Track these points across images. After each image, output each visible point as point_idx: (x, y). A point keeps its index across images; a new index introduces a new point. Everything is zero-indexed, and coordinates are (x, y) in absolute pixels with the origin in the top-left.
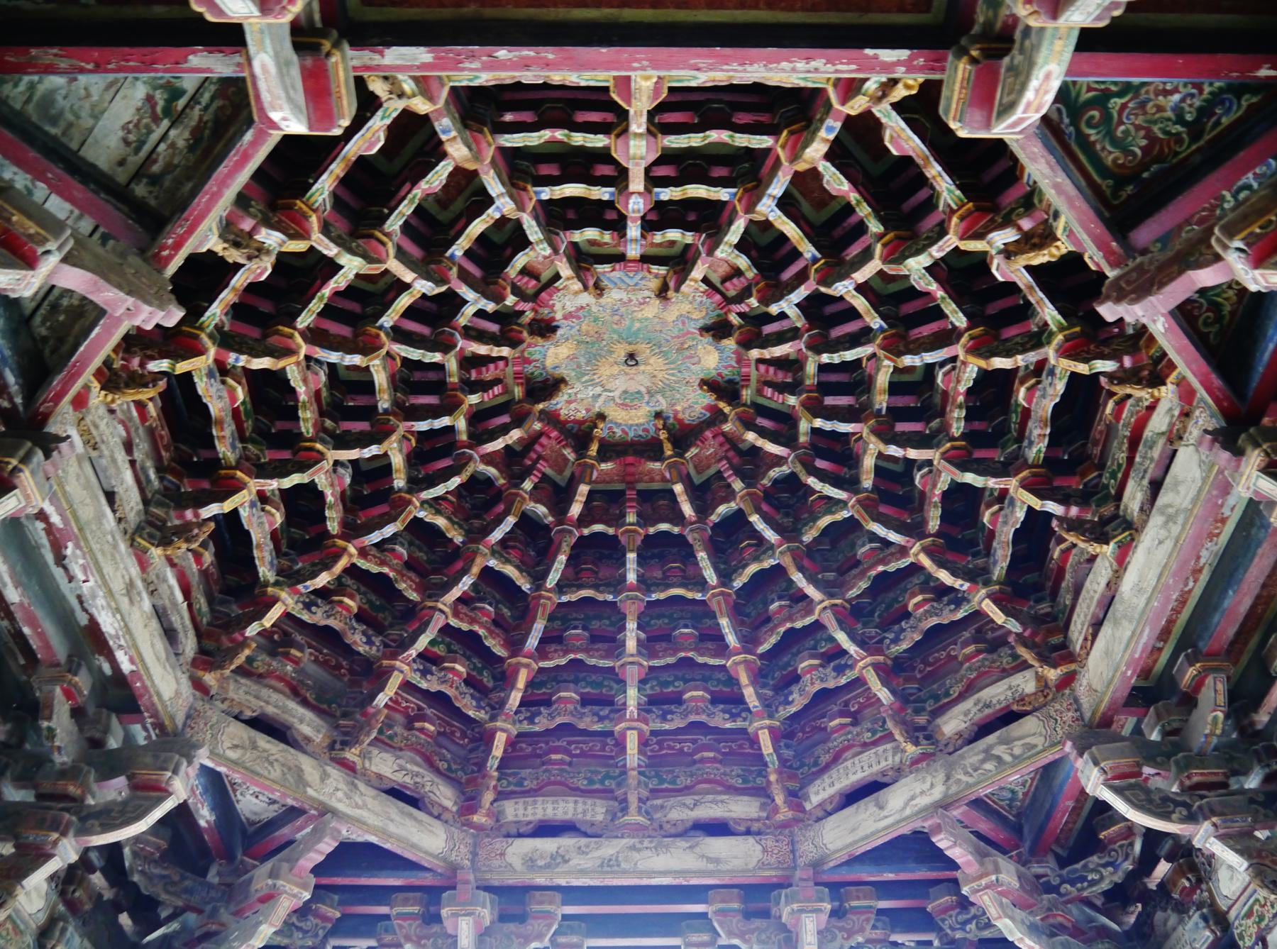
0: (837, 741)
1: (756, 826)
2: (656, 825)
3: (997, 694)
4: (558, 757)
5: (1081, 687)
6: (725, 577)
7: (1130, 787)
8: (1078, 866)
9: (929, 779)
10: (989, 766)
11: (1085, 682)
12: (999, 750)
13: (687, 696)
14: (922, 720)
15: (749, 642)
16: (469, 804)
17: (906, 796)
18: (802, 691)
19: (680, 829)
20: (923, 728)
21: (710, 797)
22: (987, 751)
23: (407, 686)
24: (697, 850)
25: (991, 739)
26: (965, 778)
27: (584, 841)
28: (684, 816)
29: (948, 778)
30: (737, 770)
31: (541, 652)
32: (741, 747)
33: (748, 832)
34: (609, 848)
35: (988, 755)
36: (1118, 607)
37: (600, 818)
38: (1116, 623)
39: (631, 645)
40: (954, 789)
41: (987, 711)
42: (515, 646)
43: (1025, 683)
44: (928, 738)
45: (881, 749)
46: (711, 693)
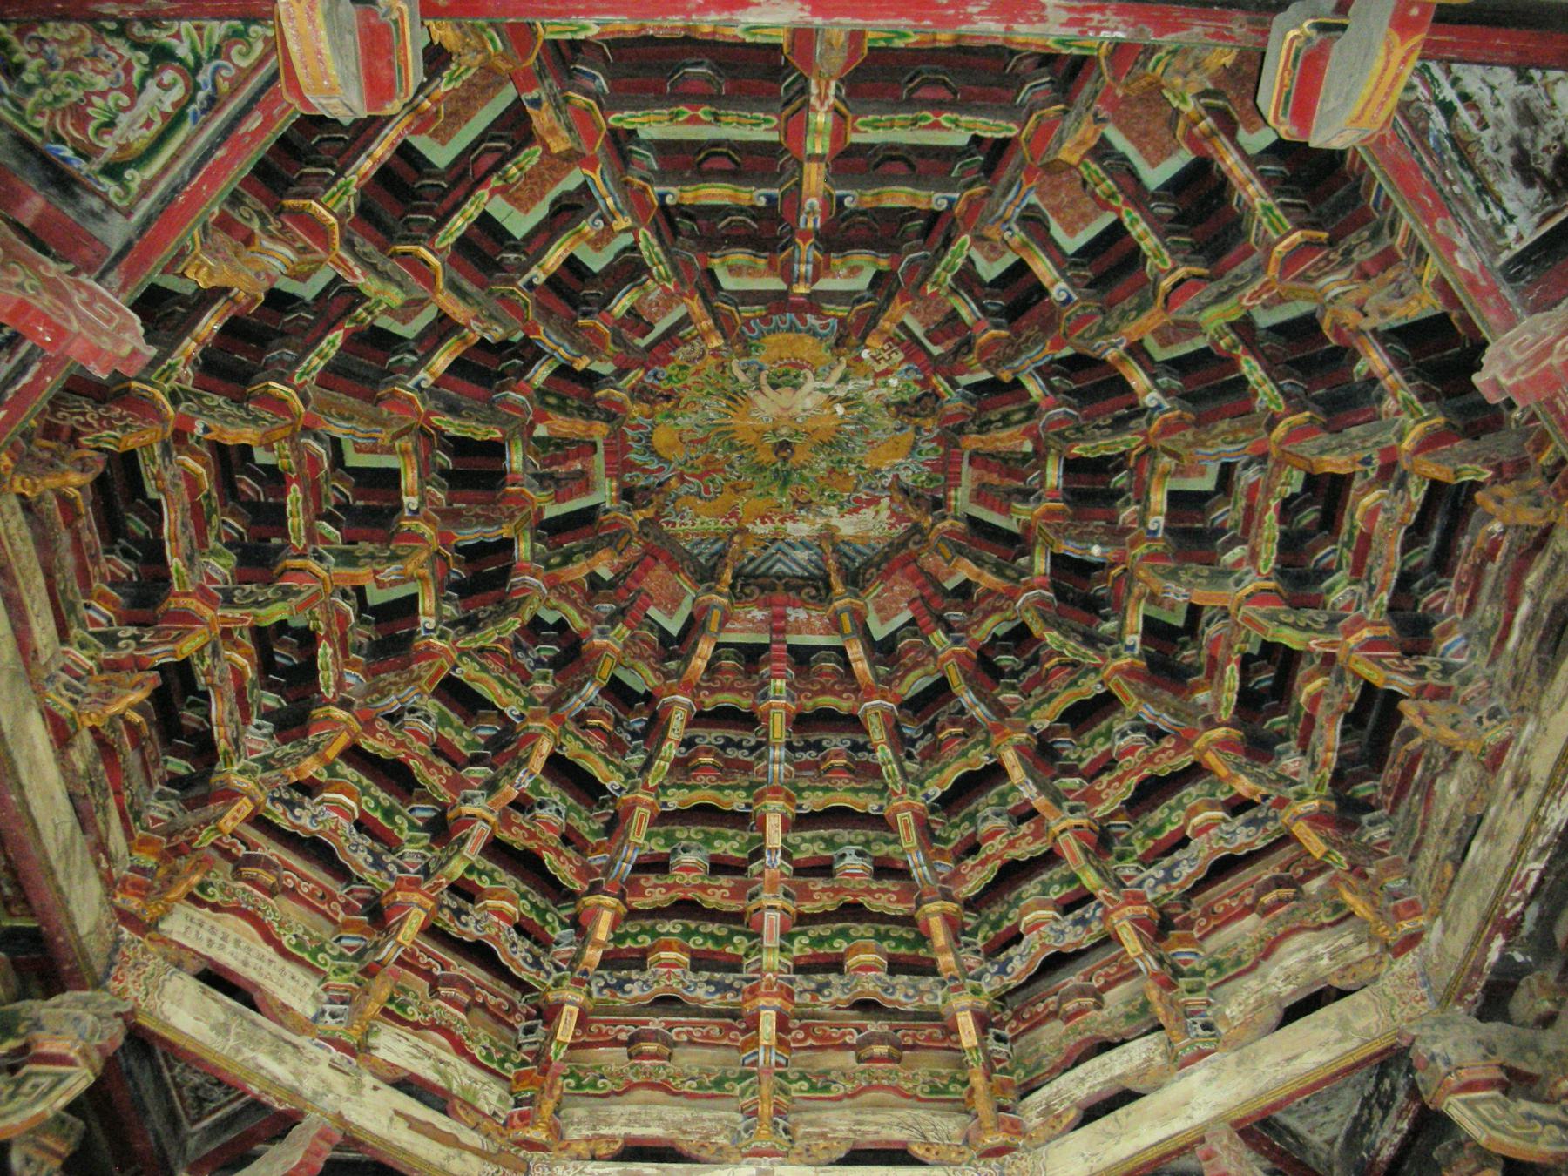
4: (651, 1047)
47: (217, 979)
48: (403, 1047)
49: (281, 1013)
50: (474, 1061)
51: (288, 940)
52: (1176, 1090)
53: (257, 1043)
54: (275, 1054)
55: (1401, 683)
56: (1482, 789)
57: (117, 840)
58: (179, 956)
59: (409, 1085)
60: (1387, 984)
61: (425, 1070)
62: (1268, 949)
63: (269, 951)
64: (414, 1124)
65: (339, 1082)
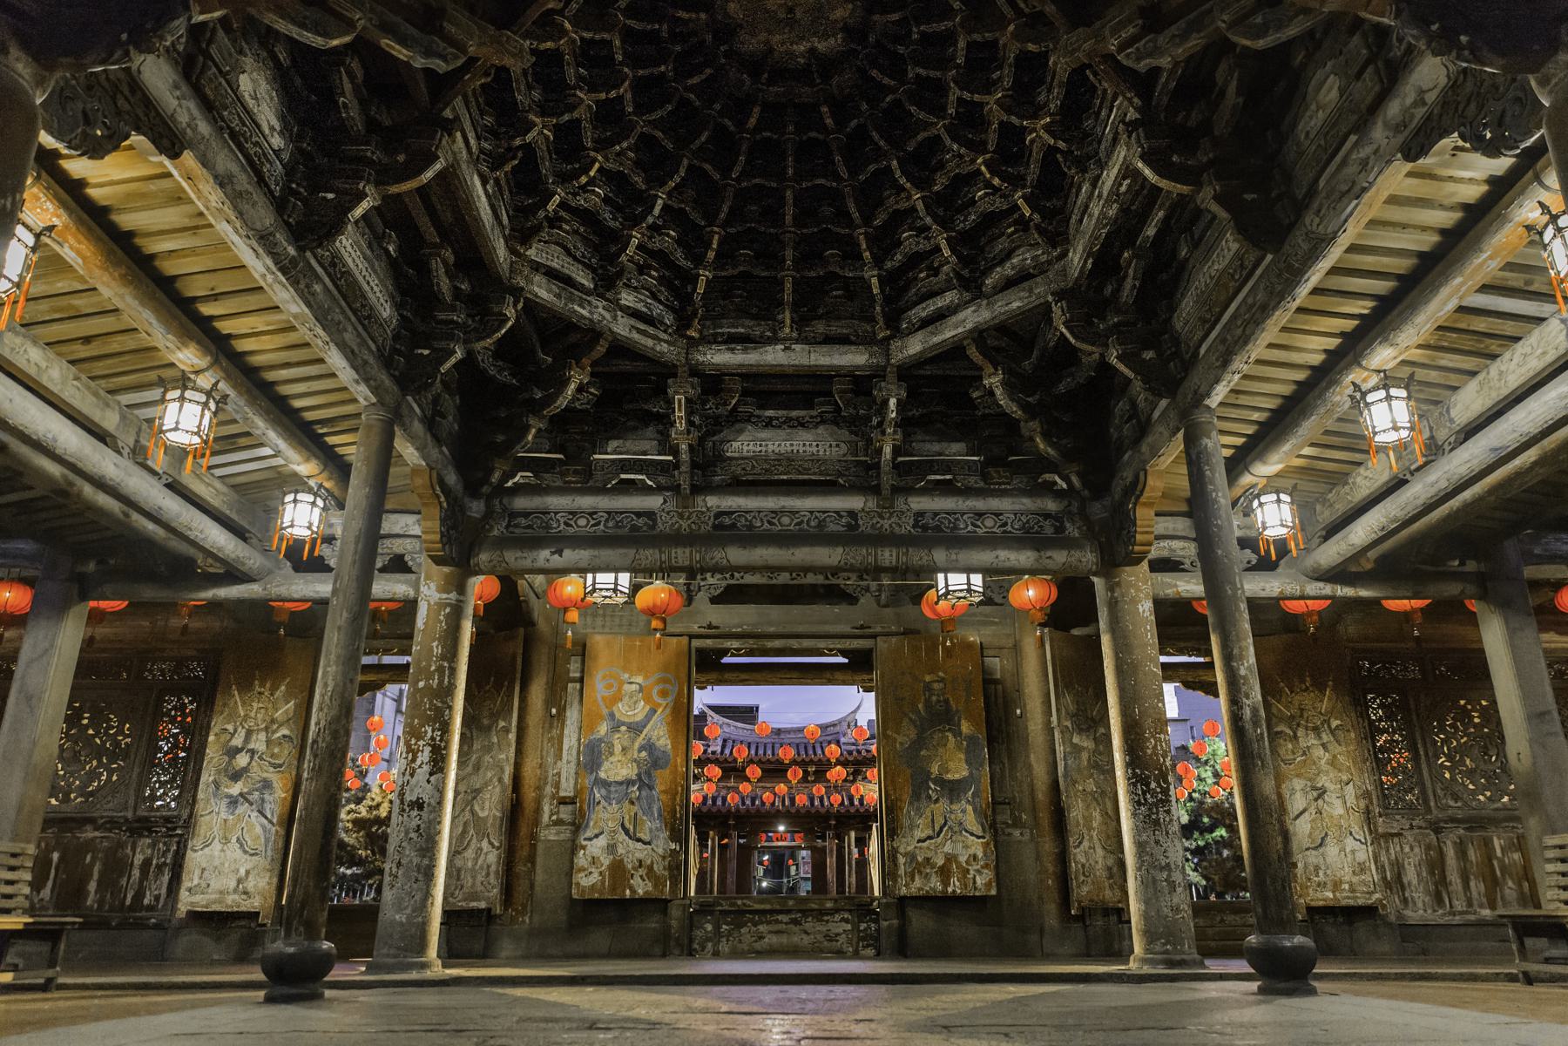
6: (853, 173)
15: (867, 220)
16: (683, 322)
23: (640, 247)
31: (726, 224)
39: (789, 219)
42: (711, 219)
47: (552, 274)
48: (631, 298)
49: (580, 288)
50: (660, 302)
51: (578, 254)
52: (961, 316)
53: (573, 301)
54: (581, 306)
55: (1061, 145)
56: (1090, 197)
57: (505, 220)
58: (536, 267)
59: (634, 314)
60: (1051, 275)
61: (641, 307)
62: (1009, 255)
63: (570, 260)
64: (639, 331)
65: (607, 315)
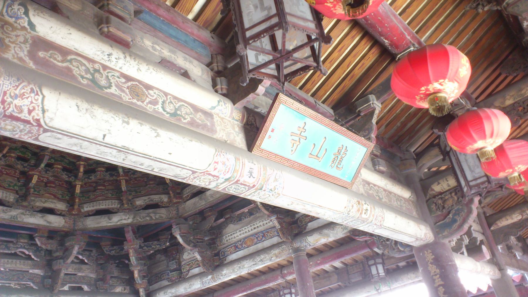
0: (98, 193)
1: (63, 213)
2: (31, 206)
3: (156, 198)
5: (181, 207)
7: (184, 236)
8: (151, 243)
9: (128, 216)
10: (148, 218)
11: (183, 206)
12: (152, 215)
13: (55, 166)
14: (130, 198)
17: (119, 219)
18: (95, 176)
19: (38, 210)
20: (130, 200)
21: (51, 200)
22: (148, 214)
24: (44, 218)
25: (151, 210)
26: (140, 219)
27: (5, 208)
28: (41, 205)
29: (134, 218)
30: (60, 192)
32: (63, 184)
33: (60, 215)
34: (14, 212)
35: (148, 215)
36: (203, 196)
37: (12, 200)
38: (201, 199)
40: (135, 221)
41: (151, 202)
43: (165, 198)
44: (131, 204)
45: (114, 201)
46: (63, 166)
